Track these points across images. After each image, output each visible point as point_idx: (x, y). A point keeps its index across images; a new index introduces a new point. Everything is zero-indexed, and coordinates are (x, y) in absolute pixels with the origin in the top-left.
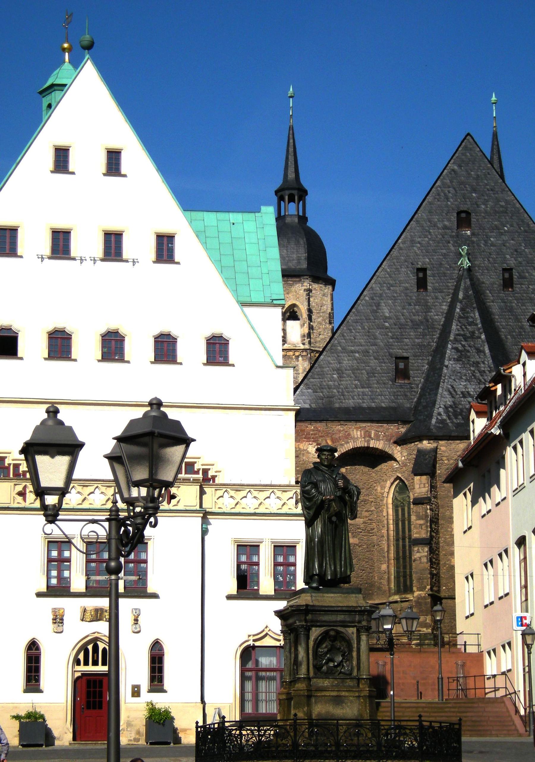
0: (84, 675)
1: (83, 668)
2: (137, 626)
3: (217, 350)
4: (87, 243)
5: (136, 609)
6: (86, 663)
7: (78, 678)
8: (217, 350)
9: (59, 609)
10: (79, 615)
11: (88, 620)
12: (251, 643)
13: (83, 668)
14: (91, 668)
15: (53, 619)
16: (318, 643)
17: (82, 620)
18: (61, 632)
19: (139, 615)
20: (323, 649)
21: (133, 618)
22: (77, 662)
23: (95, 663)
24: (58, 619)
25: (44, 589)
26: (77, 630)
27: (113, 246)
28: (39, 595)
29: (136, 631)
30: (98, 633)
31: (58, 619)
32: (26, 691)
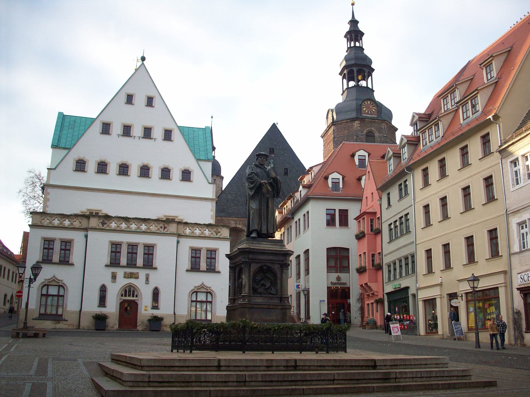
0: (125, 301)
1: (124, 298)
3: (186, 175)
4: (137, 131)
6: (125, 296)
8: (186, 175)
12: (196, 290)
13: (124, 298)
14: (127, 298)
16: (256, 273)
17: (124, 277)
20: (258, 278)
23: (129, 296)
24: (114, 277)
25: (109, 264)
26: (122, 282)
27: (147, 133)
28: (106, 266)
31: (114, 277)
32: (99, 307)
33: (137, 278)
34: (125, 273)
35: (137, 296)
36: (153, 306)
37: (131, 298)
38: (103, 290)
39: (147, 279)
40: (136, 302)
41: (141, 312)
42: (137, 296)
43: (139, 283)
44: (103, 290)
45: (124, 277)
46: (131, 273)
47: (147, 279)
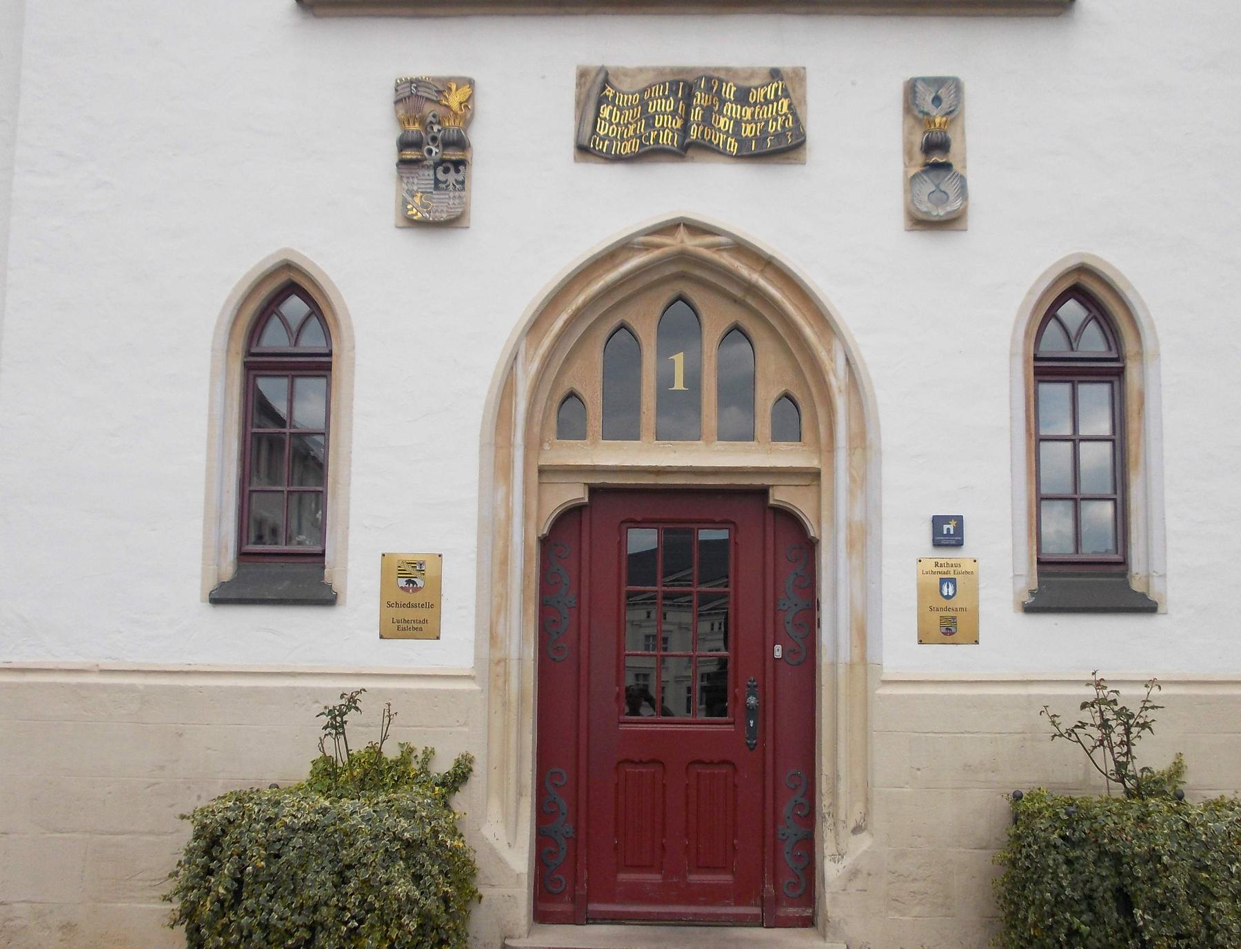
2: (949, 186)
5: (939, 82)
6: (621, 423)
7: (569, 517)
9: (442, 87)
10: (563, 126)
11: (628, 148)
14: (647, 455)
15: (404, 144)
17: (584, 150)
18: (454, 222)
19: (953, 114)
21: (919, 139)
22: (568, 414)
24: (434, 146)
26: (552, 211)
29: (940, 212)
30: (696, 229)
31: (434, 146)
33: (783, 147)
34: (597, 89)
35: (790, 419)
36: (1046, 565)
37: (707, 456)
38: (284, 341)
39: (935, 154)
40: (789, 519)
41: (864, 662)
42: (790, 419)
43: (824, 220)
44: (284, 341)
45: (584, 150)
46: (684, 86)
47: (935, 154)
